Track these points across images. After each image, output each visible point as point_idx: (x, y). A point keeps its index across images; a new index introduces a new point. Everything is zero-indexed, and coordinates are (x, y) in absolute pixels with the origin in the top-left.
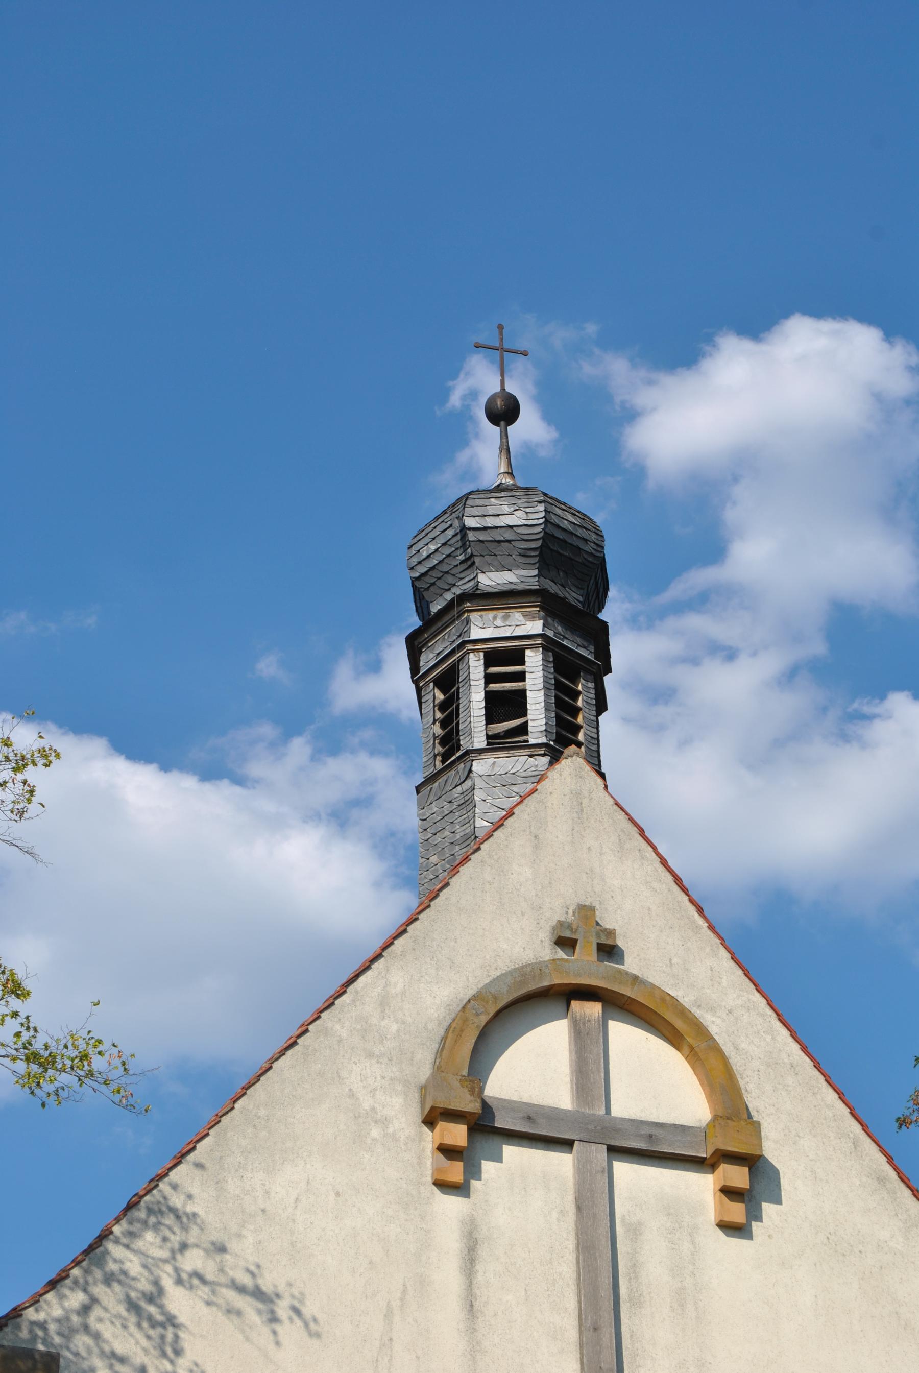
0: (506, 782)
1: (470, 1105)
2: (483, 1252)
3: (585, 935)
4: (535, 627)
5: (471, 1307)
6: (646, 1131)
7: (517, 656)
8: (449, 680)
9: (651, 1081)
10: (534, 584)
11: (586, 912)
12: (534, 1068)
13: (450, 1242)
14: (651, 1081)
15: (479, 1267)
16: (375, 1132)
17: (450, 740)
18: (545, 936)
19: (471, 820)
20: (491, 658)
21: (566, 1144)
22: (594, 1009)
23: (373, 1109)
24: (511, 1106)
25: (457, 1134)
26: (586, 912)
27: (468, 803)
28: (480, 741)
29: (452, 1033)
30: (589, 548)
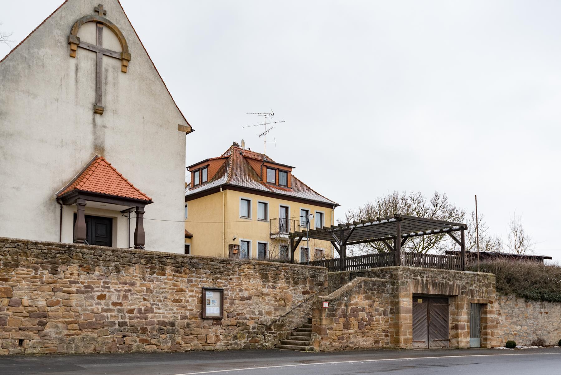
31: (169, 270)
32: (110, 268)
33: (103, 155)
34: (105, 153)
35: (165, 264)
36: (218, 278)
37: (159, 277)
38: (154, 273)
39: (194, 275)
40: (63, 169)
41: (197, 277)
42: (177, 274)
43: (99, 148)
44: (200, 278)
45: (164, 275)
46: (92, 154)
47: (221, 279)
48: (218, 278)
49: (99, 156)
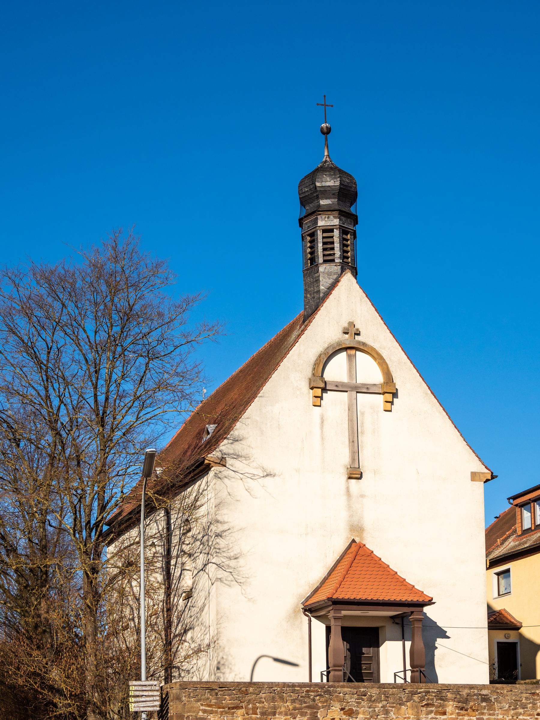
0: (329, 274)
1: (322, 385)
2: (325, 423)
3: (351, 330)
4: (336, 222)
5: (323, 439)
6: (366, 387)
7: (332, 231)
8: (313, 235)
9: (368, 371)
10: (337, 207)
11: (352, 324)
12: (337, 370)
13: (318, 421)
14: (368, 371)
15: (324, 427)
16: (298, 392)
17: (313, 259)
18: (341, 331)
19: (318, 286)
20: (324, 231)
21: (347, 391)
22: (352, 352)
23: (297, 386)
24: (332, 383)
25: (318, 392)
26: (352, 324)
27: (318, 281)
28: (321, 260)
29: (316, 364)
30: (353, 189)
31: (450, 707)
32: (377, 709)
33: (362, 538)
34: (365, 535)
35: (444, 699)
36: (520, 714)
37: (438, 717)
38: (431, 712)
39: (485, 711)
40: (311, 565)
41: (490, 715)
42: (463, 712)
43: (357, 528)
44: (494, 715)
45: (444, 713)
46: (348, 538)
47: (523, 715)
48: (520, 714)
49: (357, 540)
